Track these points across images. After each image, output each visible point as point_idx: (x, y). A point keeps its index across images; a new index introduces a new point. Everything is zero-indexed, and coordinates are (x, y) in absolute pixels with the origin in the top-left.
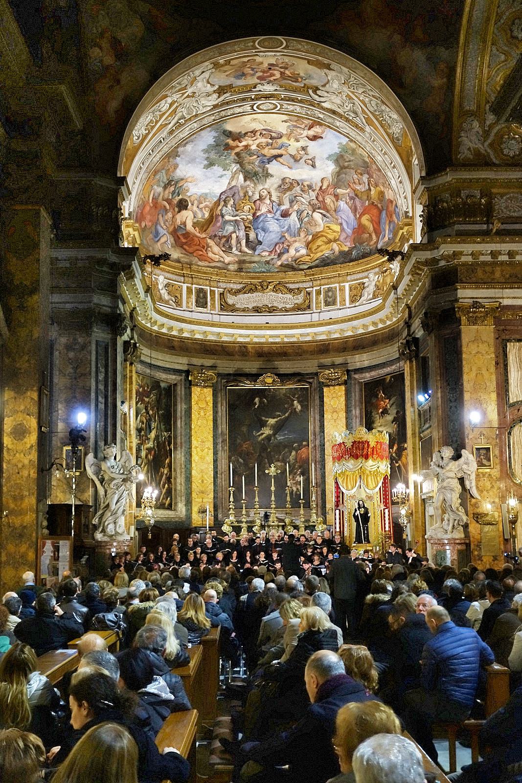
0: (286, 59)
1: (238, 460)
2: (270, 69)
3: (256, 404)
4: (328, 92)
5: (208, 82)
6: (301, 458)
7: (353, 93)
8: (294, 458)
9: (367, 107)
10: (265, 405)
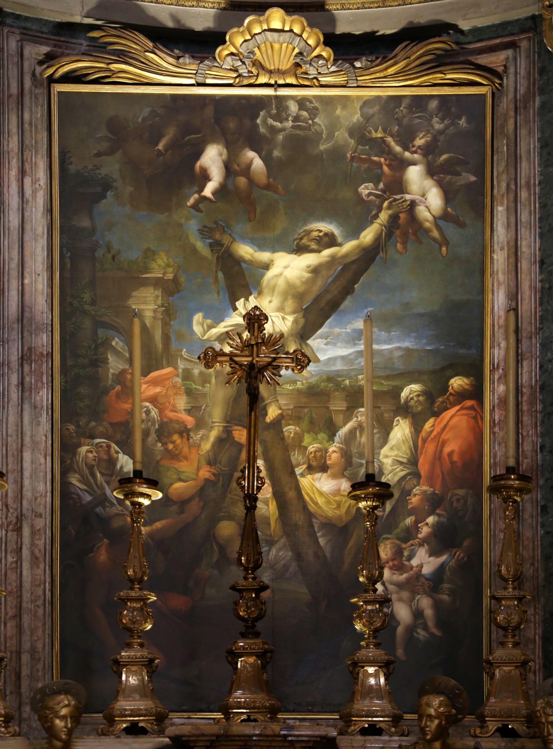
1: (112, 462)
3: (205, 177)
6: (438, 457)
8: (404, 454)
10: (251, 182)
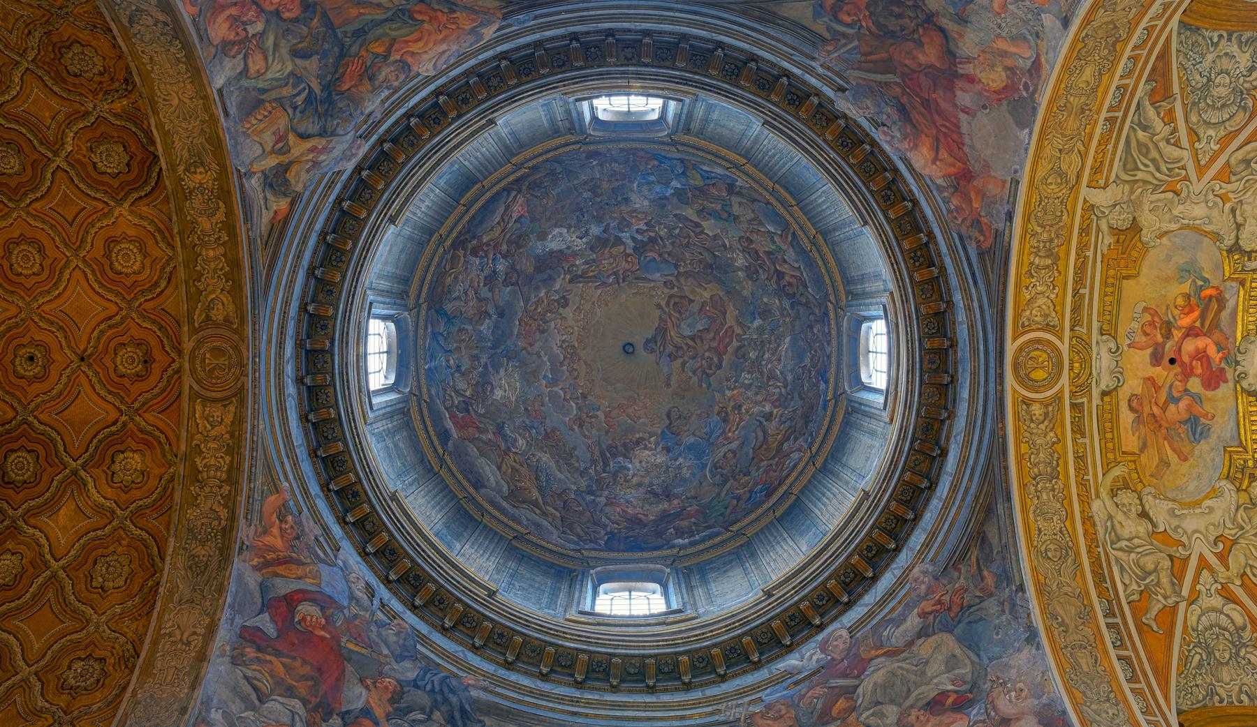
0: (1129, 324)
2: (1172, 361)
4: (1239, 227)
5: (1198, 504)
7: (1201, 170)
9: (1239, 131)
